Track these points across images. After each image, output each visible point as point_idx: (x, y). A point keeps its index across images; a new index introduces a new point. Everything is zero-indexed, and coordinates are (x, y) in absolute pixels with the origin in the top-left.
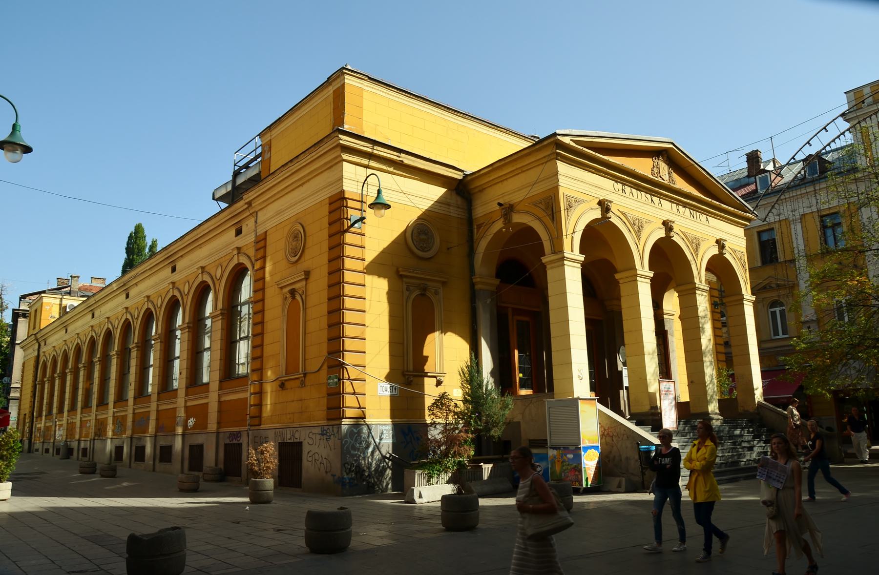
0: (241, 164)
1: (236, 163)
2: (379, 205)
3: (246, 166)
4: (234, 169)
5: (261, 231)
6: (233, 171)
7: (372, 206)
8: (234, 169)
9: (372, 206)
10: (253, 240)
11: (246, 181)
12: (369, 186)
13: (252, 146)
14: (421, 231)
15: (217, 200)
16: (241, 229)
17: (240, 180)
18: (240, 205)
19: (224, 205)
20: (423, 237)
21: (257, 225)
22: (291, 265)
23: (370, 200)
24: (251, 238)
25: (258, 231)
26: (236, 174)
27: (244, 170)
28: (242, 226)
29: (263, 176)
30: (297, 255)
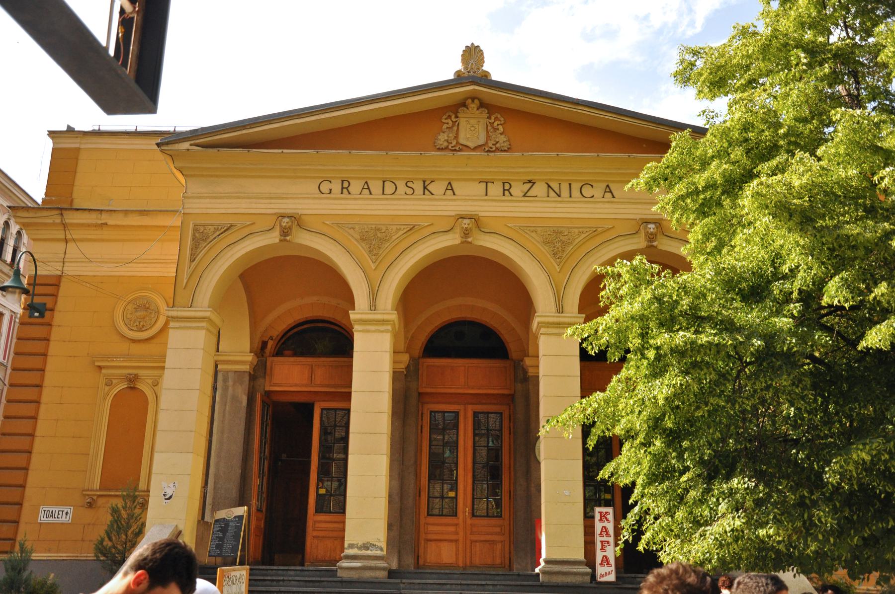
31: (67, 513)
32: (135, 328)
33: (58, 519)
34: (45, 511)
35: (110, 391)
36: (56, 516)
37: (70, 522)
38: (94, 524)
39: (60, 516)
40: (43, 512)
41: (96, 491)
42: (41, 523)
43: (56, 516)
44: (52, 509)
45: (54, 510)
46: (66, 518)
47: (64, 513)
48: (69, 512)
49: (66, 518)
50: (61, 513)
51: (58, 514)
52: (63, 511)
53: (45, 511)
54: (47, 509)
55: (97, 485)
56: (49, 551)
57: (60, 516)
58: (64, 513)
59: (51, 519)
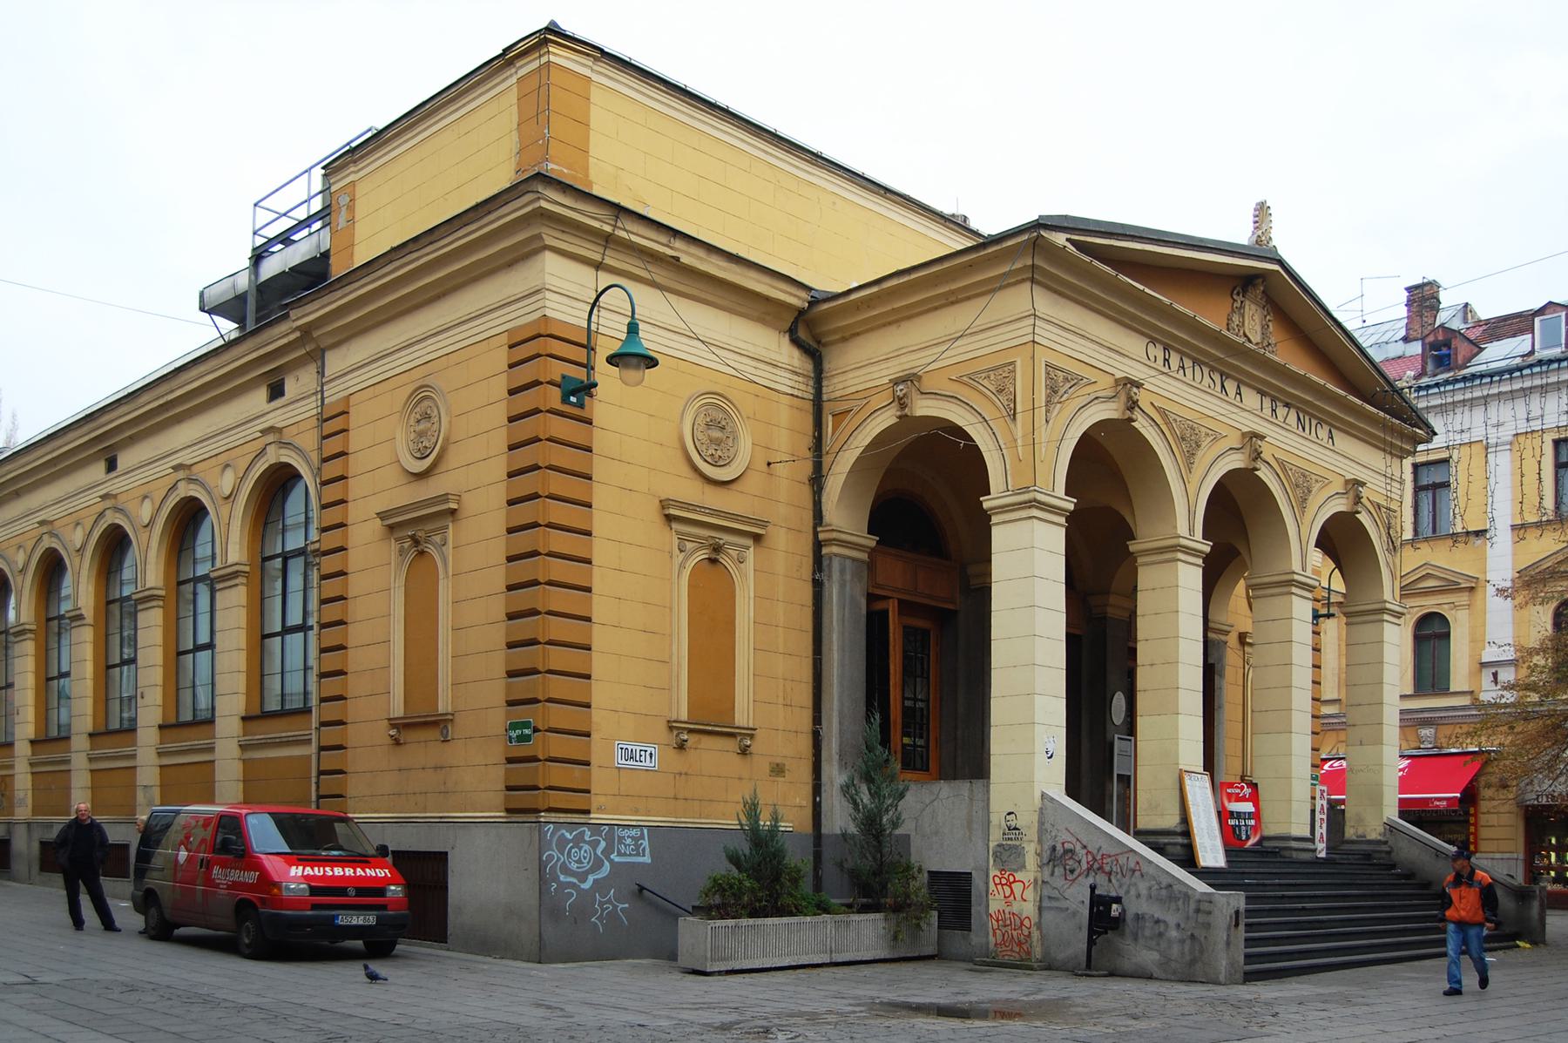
0: (272, 231)
1: (257, 228)
2: (632, 359)
3: (285, 239)
4: (254, 242)
5: (334, 393)
6: (251, 248)
7: (613, 360)
8: (254, 242)
9: (613, 360)
10: (314, 412)
11: (284, 272)
12: (603, 313)
13: (299, 191)
14: (711, 421)
15: (210, 312)
16: (283, 384)
17: (270, 268)
18: (281, 334)
19: (228, 327)
20: (716, 434)
21: (324, 380)
22: (412, 479)
23: (605, 348)
24: (310, 408)
25: (326, 394)
26: (258, 256)
27: (280, 246)
28: (283, 379)
29: (337, 269)
30: (428, 456)
31: (651, 754)
32: (709, 459)
33: (641, 764)
34: (622, 749)
35: (686, 559)
36: (638, 759)
37: (656, 769)
38: (686, 774)
39: (643, 759)
40: (620, 750)
41: (686, 722)
42: (619, 768)
43: (638, 759)
44: (634, 748)
45: (634, 748)
46: (651, 762)
47: (648, 753)
48: (653, 753)
49: (651, 762)
50: (643, 753)
51: (641, 756)
52: (646, 751)
53: (622, 749)
54: (625, 747)
55: (684, 716)
56: (636, 812)
57: (643, 759)
58: (648, 753)
59: (631, 762)
